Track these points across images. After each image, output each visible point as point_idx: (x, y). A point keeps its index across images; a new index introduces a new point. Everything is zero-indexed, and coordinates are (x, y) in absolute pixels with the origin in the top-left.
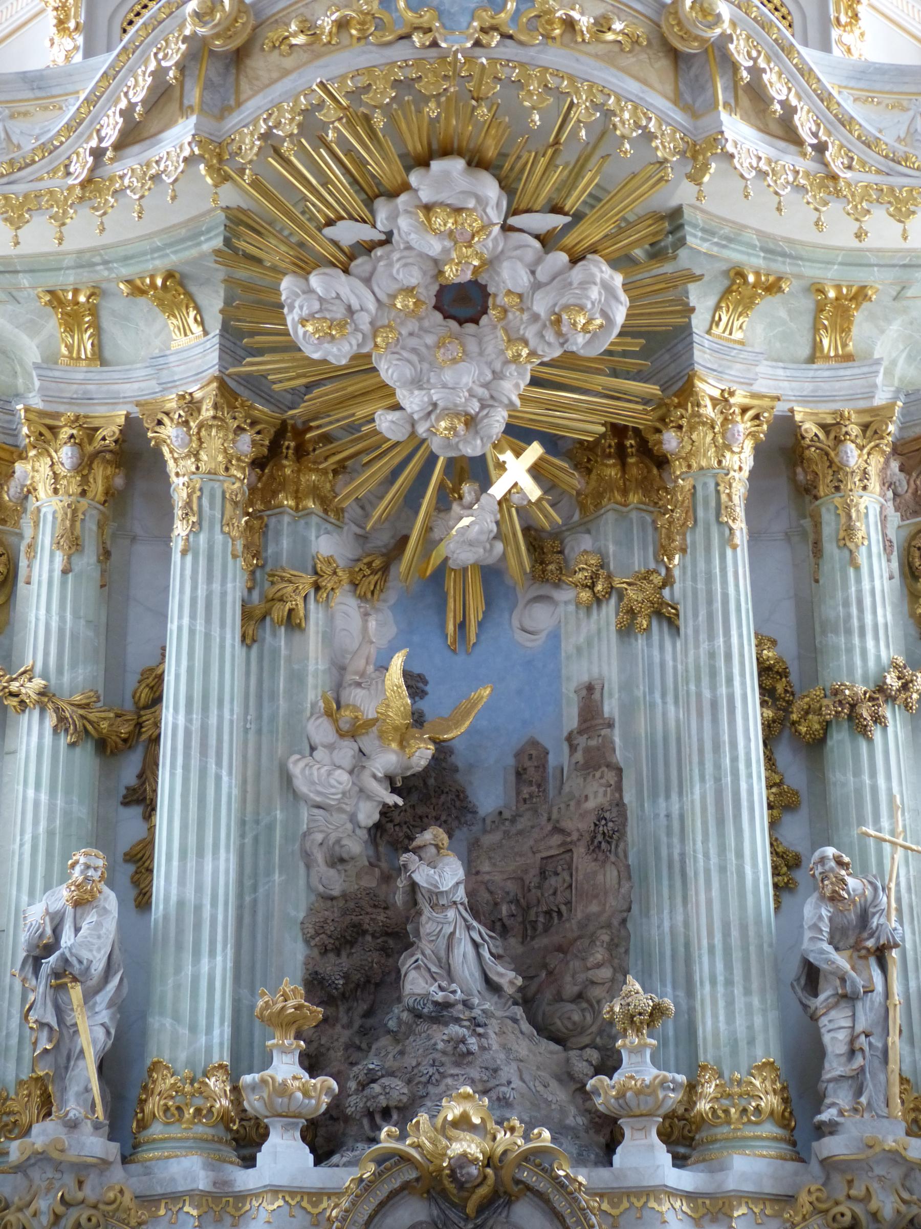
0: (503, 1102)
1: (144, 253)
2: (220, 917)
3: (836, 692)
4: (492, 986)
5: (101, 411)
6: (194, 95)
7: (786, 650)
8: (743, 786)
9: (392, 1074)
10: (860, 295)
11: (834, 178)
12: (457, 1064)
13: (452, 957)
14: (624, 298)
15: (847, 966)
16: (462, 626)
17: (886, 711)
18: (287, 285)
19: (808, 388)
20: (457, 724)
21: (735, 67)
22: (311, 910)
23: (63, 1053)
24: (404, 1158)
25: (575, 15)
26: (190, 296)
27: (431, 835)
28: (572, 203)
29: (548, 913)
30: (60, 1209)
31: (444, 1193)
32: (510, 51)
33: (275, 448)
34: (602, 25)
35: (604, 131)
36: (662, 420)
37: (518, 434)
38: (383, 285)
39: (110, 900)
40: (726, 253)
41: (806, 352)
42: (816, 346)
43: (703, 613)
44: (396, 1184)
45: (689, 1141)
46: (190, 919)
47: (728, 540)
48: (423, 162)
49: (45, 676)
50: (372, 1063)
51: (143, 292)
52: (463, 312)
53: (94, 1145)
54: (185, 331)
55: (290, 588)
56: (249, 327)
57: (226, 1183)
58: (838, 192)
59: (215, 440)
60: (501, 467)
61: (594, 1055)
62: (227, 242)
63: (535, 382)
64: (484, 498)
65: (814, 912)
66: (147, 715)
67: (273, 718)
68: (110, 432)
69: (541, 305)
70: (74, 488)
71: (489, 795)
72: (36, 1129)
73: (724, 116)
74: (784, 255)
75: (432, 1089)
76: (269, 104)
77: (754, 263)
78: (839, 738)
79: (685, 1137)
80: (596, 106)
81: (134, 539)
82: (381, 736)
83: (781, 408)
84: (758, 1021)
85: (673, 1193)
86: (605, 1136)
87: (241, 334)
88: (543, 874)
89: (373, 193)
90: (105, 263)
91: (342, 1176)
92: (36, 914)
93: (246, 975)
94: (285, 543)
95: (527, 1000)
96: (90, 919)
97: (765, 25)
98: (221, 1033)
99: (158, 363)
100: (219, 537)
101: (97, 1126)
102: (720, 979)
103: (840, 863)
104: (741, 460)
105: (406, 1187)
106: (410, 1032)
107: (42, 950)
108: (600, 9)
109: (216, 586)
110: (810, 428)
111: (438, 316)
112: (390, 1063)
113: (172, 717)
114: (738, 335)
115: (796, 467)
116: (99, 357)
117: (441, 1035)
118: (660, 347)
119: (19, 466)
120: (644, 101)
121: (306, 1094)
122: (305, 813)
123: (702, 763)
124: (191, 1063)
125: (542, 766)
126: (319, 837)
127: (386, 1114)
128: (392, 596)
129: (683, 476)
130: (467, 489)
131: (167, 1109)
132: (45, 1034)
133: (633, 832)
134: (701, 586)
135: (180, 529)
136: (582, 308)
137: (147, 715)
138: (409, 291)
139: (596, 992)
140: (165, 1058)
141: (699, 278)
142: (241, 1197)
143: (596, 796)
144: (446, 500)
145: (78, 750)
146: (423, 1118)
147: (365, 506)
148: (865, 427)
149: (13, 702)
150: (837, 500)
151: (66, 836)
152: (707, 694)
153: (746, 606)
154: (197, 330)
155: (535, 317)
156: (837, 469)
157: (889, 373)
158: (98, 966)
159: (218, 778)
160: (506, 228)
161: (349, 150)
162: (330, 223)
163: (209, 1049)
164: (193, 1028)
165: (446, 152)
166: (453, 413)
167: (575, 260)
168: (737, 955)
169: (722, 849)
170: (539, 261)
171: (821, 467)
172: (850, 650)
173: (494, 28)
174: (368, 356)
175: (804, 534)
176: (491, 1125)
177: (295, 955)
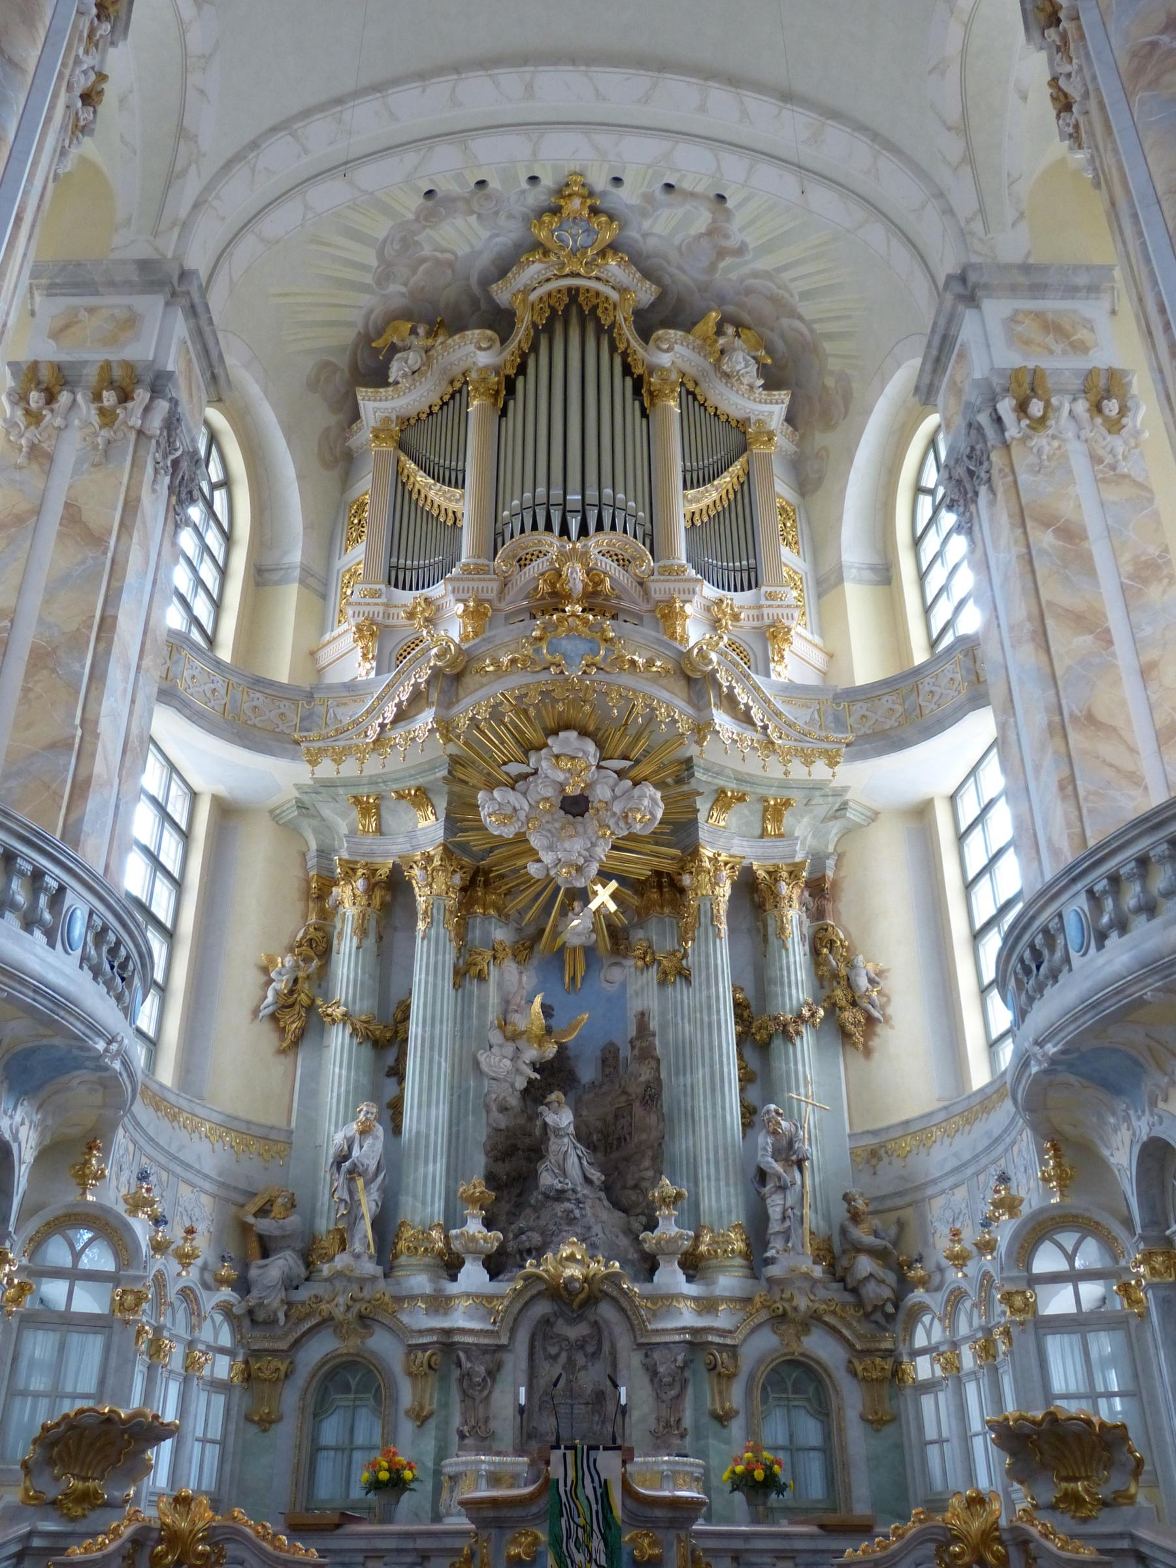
0: (593, 1246)
2: (439, 1142)
3: (776, 1018)
4: (588, 1180)
5: (379, 860)
6: (434, 696)
7: (749, 994)
9: (531, 1229)
10: (787, 803)
11: (773, 743)
13: (568, 1164)
14: (661, 804)
15: (781, 1170)
16: (573, 979)
17: (803, 1029)
18: (481, 796)
19: (760, 851)
21: (720, 686)
22: (489, 1137)
23: (353, 1216)
24: (539, 1278)
25: (636, 658)
26: (428, 799)
27: (555, 1096)
28: (635, 754)
29: (619, 1139)
31: (560, 1297)
32: (602, 676)
34: (650, 663)
35: (651, 719)
36: (682, 868)
37: (605, 876)
38: (533, 796)
39: (379, 1130)
41: (759, 832)
42: (764, 829)
44: (534, 1291)
45: (695, 1267)
46: (423, 1142)
47: (717, 934)
48: (555, 732)
49: (346, 1005)
51: (403, 797)
53: (369, 1268)
54: (426, 818)
56: (460, 817)
58: (774, 751)
59: (441, 877)
60: (595, 893)
61: (643, 1219)
62: (450, 772)
63: (614, 848)
65: (765, 1141)
66: (400, 1027)
67: (470, 1029)
69: (617, 808)
70: (364, 902)
71: (587, 1073)
72: (337, 1258)
73: (714, 711)
75: (555, 1239)
76: (472, 705)
78: (777, 1043)
79: (693, 1265)
80: (647, 706)
81: (396, 929)
82: (529, 1040)
83: (746, 862)
84: (733, 1201)
85: (686, 1297)
86: (648, 1266)
87: (457, 821)
88: (616, 1117)
89: (528, 748)
91: (505, 1287)
92: (339, 1138)
93: (454, 1173)
94: (478, 932)
95: (607, 1188)
96: (368, 1142)
97: (736, 664)
98: (439, 1206)
99: (411, 834)
100: (442, 931)
101: (371, 1257)
104: (725, 891)
105: (540, 1293)
107: (342, 1158)
108: (649, 655)
109: (440, 957)
110: (761, 873)
112: (531, 1223)
113: (415, 1029)
114: (722, 823)
115: (754, 895)
116: (379, 831)
117: (560, 1208)
118: (681, 831)
119: (334, 889)
120: (673, 705)
122: (486, 1082)
124: (422, 1223)
125: (616, 1057)
126: (494, 1096)
127: (529, 1252)
128: (535, 962)
130: (576, 904)
133: (665, 1095)
134: (703, 959)
135: (421, 926)
136: (639, 810)
137: (400, 1027)
138: (547, 799)
139: (645, 1184)
140: (408, 1219)
143: (646, 1074)
144: (565, 910)
146: (549, 1255)
147: (521, 913)
148: (791, 873)
149: (328, 1019)
150: (776, 912)
152: (706, 1019)
153: (727, 971)
154: (433, 818)
155: (614, 814)
156: (776, 897)
157: (803, 843)
158: (373, 1167)
159: (439, 1063)
160: (599, 767)
161: (516, 727)
162: (505, 763)
164: (424, 1203)
165: (567, 727)
167: (636, 784)
168: (722, 1165)
169: (714, 1105)
170: (616, 785)
171: (767, 894)
172: (783, 995)
173: (594, 664)
175: (758, 930)
176: (587, 1259)
177: (479, 1161)
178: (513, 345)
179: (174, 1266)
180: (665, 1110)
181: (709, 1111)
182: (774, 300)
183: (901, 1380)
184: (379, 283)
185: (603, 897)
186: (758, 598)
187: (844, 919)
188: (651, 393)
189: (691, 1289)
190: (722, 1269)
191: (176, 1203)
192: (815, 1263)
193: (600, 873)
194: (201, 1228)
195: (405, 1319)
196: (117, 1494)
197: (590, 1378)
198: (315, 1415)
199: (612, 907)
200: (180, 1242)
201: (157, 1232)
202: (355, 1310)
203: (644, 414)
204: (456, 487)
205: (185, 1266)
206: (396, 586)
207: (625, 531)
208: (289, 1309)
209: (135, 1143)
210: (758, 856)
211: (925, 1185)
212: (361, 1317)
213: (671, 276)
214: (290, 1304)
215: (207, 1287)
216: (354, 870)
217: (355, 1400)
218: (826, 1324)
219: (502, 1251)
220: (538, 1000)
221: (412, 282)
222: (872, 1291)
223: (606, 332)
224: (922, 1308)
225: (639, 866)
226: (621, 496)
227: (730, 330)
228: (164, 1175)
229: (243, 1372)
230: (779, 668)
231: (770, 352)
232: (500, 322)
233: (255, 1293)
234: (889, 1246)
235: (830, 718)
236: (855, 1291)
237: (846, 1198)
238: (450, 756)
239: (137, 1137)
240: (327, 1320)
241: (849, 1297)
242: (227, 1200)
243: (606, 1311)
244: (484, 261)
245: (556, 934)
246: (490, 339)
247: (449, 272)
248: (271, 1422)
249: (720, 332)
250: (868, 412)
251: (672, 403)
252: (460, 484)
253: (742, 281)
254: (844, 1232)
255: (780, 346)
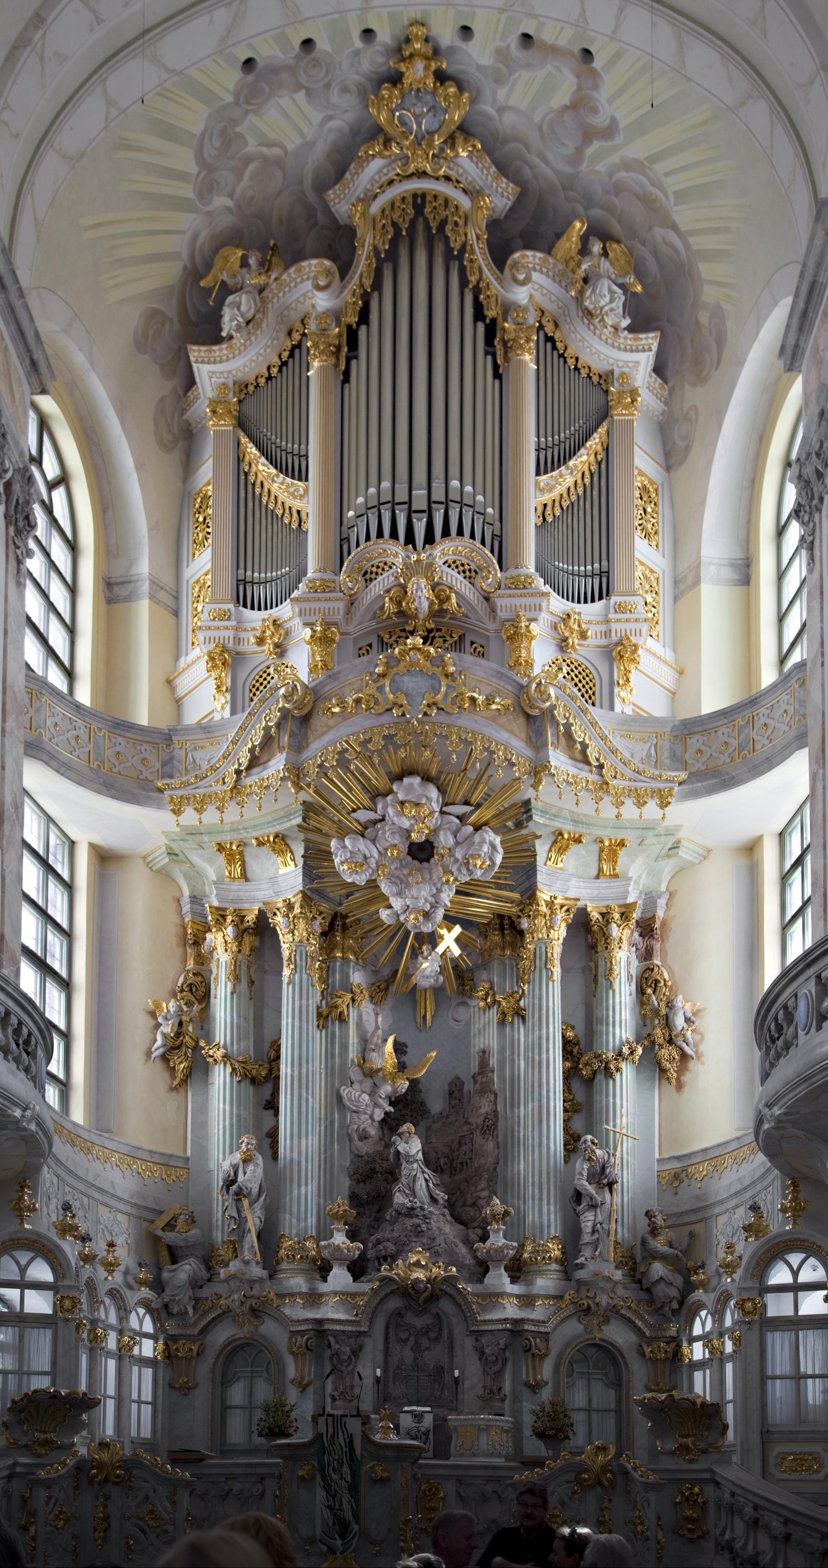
1: (263, 824)
8: (552, 1104)
9: (388, 1240)
12: (417, 1236)
20: (420, 1071)
27: (407, 1127)
30: (243, 1299)
33: (332, 925)
36: (521, 911)
39: (260, 1160)
40: (553, 823)
43: (537, 1016)
45: (520, 1270)
46: (296, 1168)
47: (550, 977)
49: (225, 1047)
50: (378, 1235)
52: (422, 857)
55: (340, 1001)
57: (314, 1289)
61: (479, 1231)
63: (458, 892)
64: (433, 954)
65: (582, 1167)
68: (251, 918)
72: (231, 1264)
74: (582, 823)
75: (406, 1248)
77: (568, 828)
79: (518, 1270)
84: (552, 1217)
85: (511, 1295)
86: (482, 1268)
90: (245, 829)
91: (365, 1287)
92: (226, 1165)
98: (312, 1221)
102: (537, 1197)
103: (593, 1143)
106: (396, 1221)
107: (230, 1182)
109: (304, 1002)
111: (409, 858)
112: (387, 1235)
113: (285, 1069)
114: (560, 865)
117: (409, 1222)
118: (521, 873)
121: (348, 1250)
123: (533, 1093)
124: (298, 1235)
127: (385, 1258)
129: (530, 943)
131: (288, 1256)
132: (233, 1222)
133: (501, 1125)
134: (536, 1002)
139: (482, 1202)
141: (540, 837)
142: (321, 1295)
144: (415, 953)
145: (243, 1084)
149: (210, 1060)
151: (239, 1126)
152: (537, 1058)
163: (306, 1228)
166: (417, 910)
174: (375, 880)
178: (353, 283)
179: (102, 1273)
180: (500, 1139)
181: (536, 1141)
182: (647, 201)
183: (681, 1360)
184: (201, 197)
185: (449, 941)
186: (607, 607)
187: (669, 946)
188: (505, 343)
189: (515, 1289)
190: (541, 1273)
191: (98, 1222)
192: (617, 1267)
193: (446, 917)
194: (120, 1241)
195: (287, 1311)
196: (66, 1441)
197: (434, 1356)
198: (222, 1384)
199: (456, 951)
200: (105, 1254)
201: (84, 1247)
202: (248, 1305)
203: (497, 375)
204: (300, 479)
205: (111, 1272)
206: (245, 606)
207: (472, 536)
208: (196, 1304)
209: (58, 1176)
210: (592, 896)
211: (713, 1205)
212: (253, 1310)
213: (532, 167)
214: (197, 1300)
215: (131, 1288)
216: (224, 917)
217: (252, 1372)
218: (622, 1316)
219: (363, 1257)
220: (391, 1040)
221: (238, 191)
222: (660, 1290)
223: (457, 258)
224: (701, 1306)
225: (482, 907)
226: (468, 489)
227: (596, 247)
228: (86, 1200)
229: (164, 1351)
230: (623, 694)
231: (640, 276)
232: (338, 244)
233: (168, 1291)
234: (680, 1254)
235: (666, 754)
236: (648, 1290)
237: (648, 1214)
238: (304, 803)
239: (59, 1171)
240: (226, 1312)
241: (643, 1295)
242: (139, 1218)
243: (445, 1305)
244: (317, 156)
245: (408, 977)
246: (328, 273)
247: (279, 174)
248: (189, 1389)
249: (584, 251)
250: (741, 363)
251: (527, 357)
252: (302, 475)
253: (611, 175)
254: (644, 1242)
255: (652, 266)
